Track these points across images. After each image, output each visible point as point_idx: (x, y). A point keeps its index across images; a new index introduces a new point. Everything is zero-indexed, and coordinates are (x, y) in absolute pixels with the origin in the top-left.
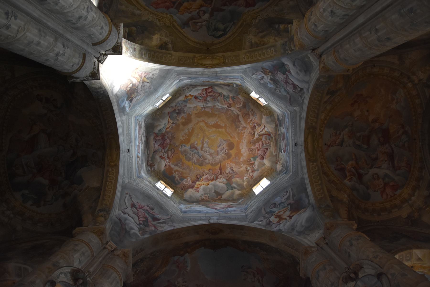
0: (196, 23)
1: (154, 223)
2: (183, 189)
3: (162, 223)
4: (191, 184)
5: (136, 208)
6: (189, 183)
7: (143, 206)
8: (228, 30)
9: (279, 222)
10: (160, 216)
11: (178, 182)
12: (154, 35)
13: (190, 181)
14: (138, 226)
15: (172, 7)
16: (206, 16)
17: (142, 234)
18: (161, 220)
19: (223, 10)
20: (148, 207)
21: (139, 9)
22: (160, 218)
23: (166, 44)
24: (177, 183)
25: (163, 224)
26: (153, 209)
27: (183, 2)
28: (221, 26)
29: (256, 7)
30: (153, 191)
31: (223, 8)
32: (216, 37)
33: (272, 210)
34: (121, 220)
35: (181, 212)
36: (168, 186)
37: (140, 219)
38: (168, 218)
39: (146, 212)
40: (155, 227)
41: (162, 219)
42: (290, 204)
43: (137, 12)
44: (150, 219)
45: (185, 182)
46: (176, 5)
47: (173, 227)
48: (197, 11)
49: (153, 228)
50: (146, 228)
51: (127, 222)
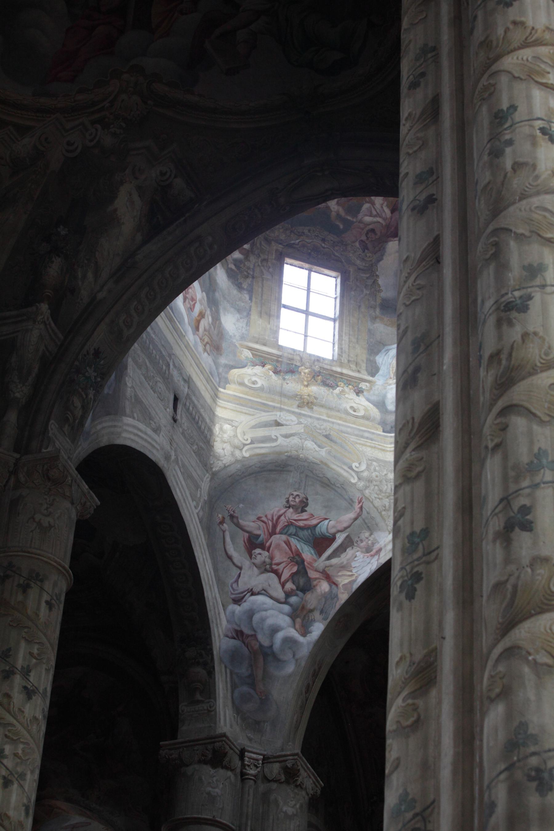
1: (321, 563)
2: (370, 246)
3: (342, 548)
4: (391, 218)
5: (262, 546)
6: (384, 215)
7: (275, 518)
10: (332, 523)
11: (343, 220)
13: (382, 207)
14: (286, 608)
17: (304, 634)
18: (337, 536)
20: (289, 507)
22: (333, 531)
24: (341, 227)
25: (345, 551)
26: (303, 506)
34: (242, 632)
35: (384, 431)
36: (316, 267)
37: (283, 579)
38: (356, 519)
39: (290, 535)
40: (328, 578)
41: (339, 531)
44: (307, 553)
45: (367, 215)
47: (376, 557)
49: (324, 587)
50: (309, 596)
51: (256, 618)
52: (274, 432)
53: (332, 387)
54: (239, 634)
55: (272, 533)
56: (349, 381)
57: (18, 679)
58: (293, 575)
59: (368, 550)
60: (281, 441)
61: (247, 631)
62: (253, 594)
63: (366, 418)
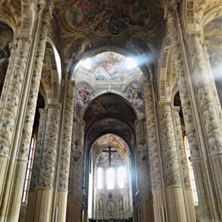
0: (102, 26)
1: (88, 96)
8: (119, 32)
9: (133, 97)
12: (82, 46)
14: (83, 102)
15: (89, 21)
16: (108, 20)
17: (85, 105)
19: (117, 19)
21: (73, 33)
23: (88, 45)
26: (86, 88)
27: (95, 15)
28: (116, 29)
29: (136, 26)
30: (84, 76)
31: (117, 18)
32: (113, 34)
33: (131, 89)
40: (88, 98)
42: (137, 91)
43: (72, 35)
44: (86, 95)
46: (91, 20)
48: (102, 19)
49: (88, 99)
51: (79, 102)
52: (83, 78)
53: (90, 72)
54: (77, 104)
55: (82, 91)
56: (92, 72)
57: (71, 111)
58: (84, 98)
59: (93, 95)
60: (84, 79)
61: (78, 104)
62: (79, 99)
63: (94, 78)
